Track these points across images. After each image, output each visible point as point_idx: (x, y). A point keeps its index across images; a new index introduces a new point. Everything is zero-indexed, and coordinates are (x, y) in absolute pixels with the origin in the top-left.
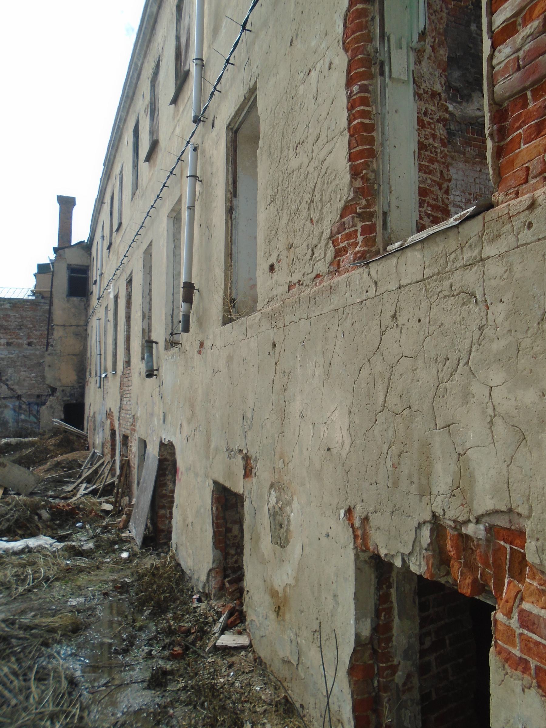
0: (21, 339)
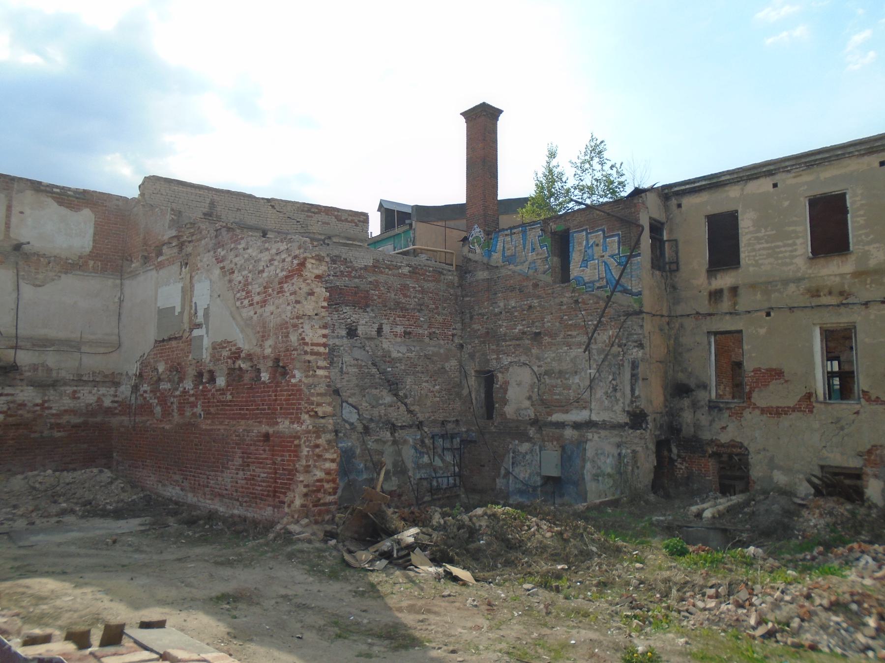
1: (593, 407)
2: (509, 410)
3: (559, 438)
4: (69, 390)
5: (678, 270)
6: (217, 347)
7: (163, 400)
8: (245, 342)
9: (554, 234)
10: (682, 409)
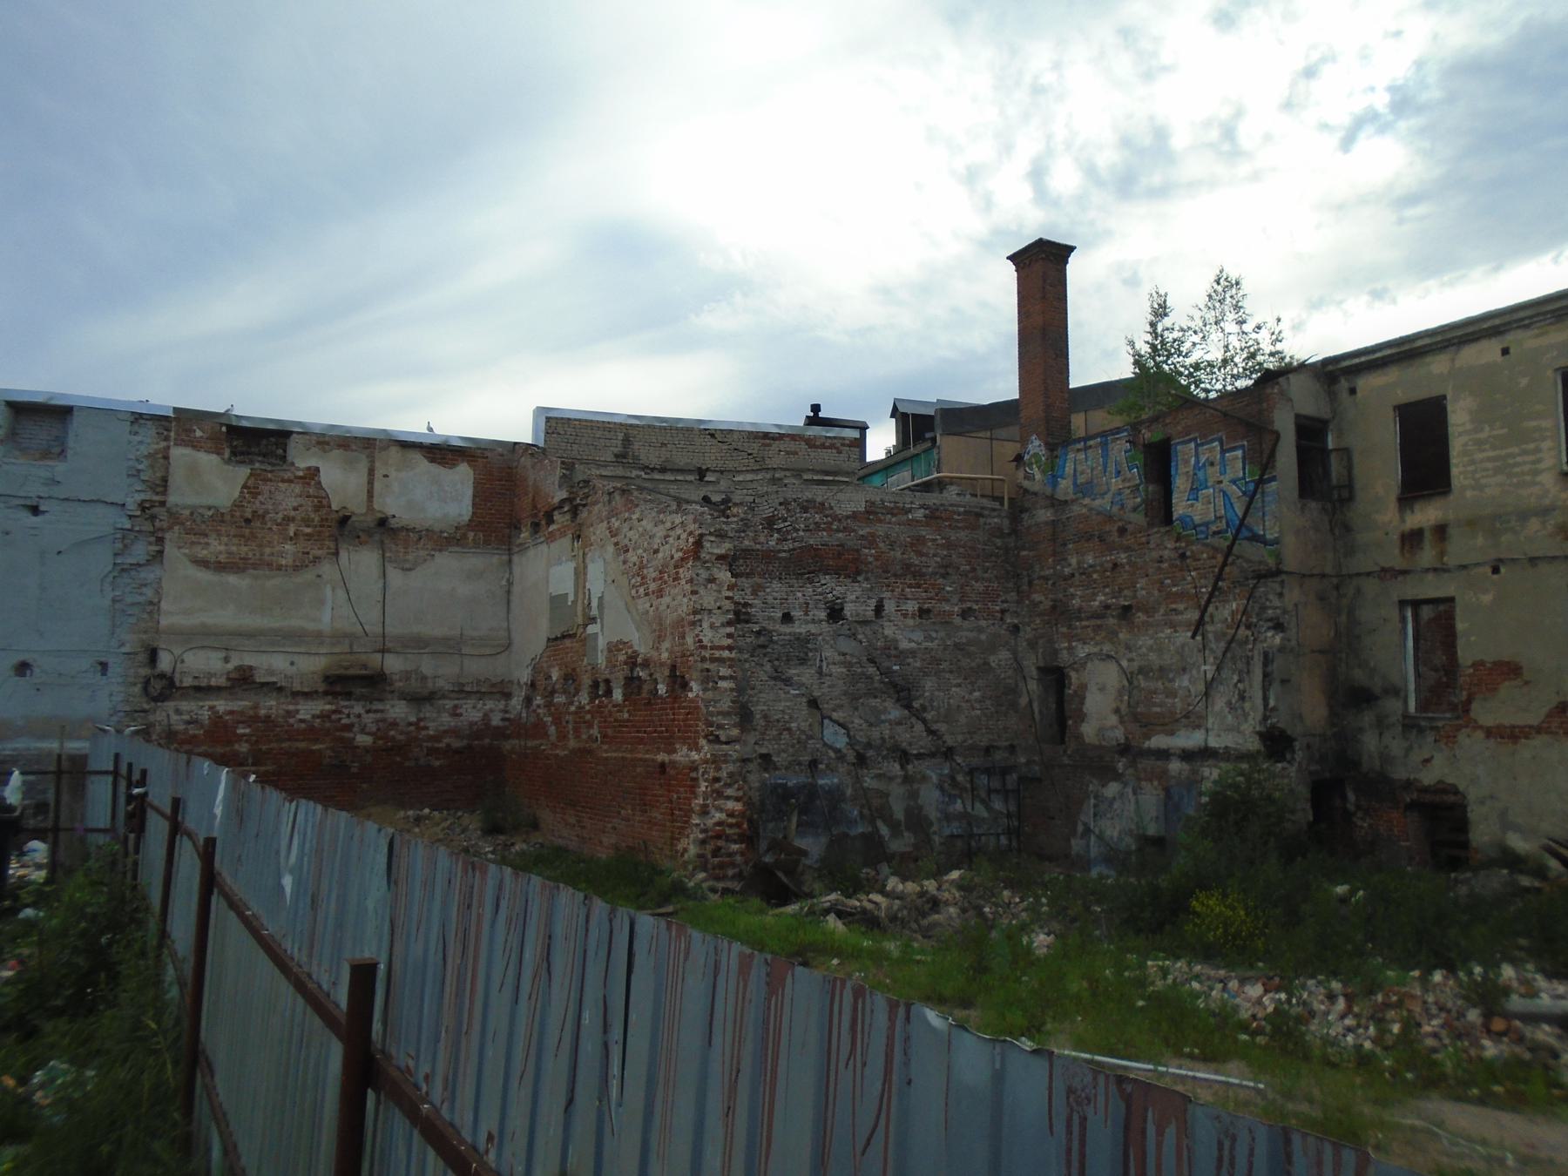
0: (947, 601)
1: (1210, 725)
2: (1088, 730)
3: (1163, 775)
4: (449, 704)
5: (1351, 498)
6: (613, 648)
7: (557, 721)
8: (641, 644)
9: (1149, 448)
10: (1361, 730)
